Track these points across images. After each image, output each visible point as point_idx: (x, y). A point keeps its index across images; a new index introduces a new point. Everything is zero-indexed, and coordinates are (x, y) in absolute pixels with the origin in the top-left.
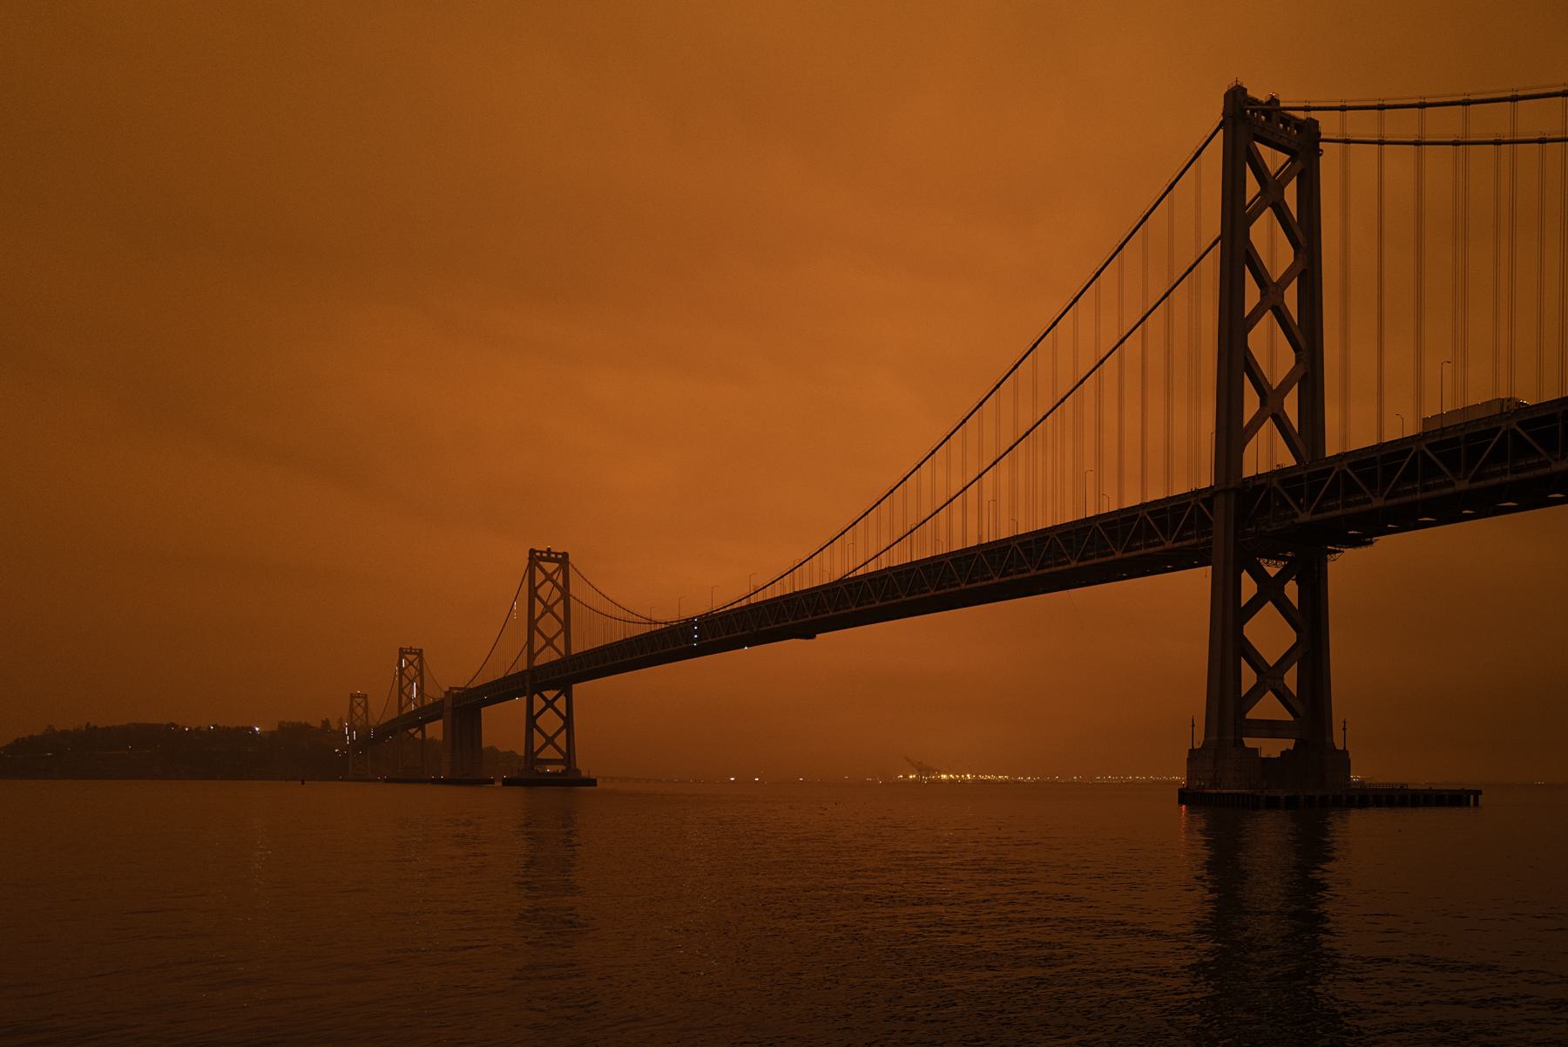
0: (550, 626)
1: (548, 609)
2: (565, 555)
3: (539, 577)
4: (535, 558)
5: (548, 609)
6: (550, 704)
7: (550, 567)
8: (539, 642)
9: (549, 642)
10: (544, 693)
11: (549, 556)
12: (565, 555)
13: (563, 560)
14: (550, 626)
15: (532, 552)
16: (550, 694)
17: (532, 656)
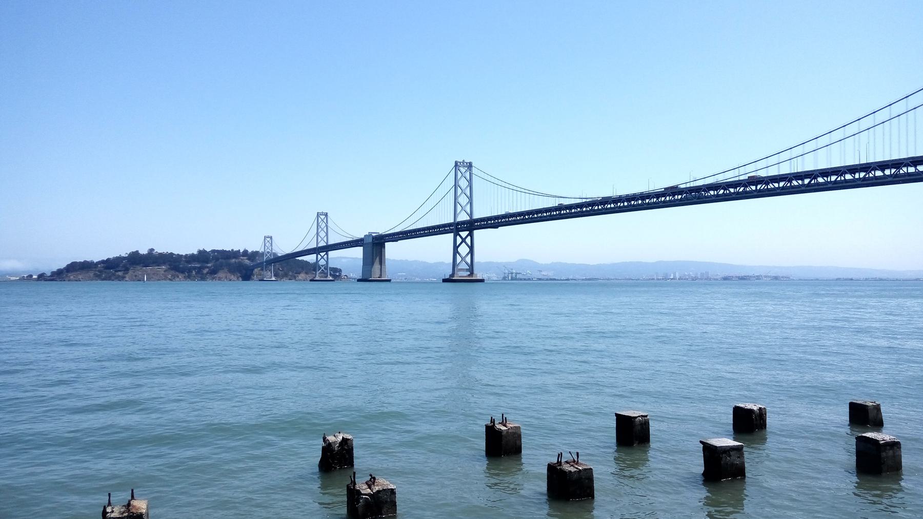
0: (322, 234)
1: (322, 230)
2: (327, 213)
3: (320, 220)
4: (318, 215)
5: (322, 230)
6: (322, 257)
7: (323, 217)
8: (320, 239)
9: (322, 239)
10: (320, 254)
11: (322, 214)
12: (327, 213)
13: (326, 215)
14: (322, 234)
15: (318, 213)
16: (322, 254)
17: (317, 243)
